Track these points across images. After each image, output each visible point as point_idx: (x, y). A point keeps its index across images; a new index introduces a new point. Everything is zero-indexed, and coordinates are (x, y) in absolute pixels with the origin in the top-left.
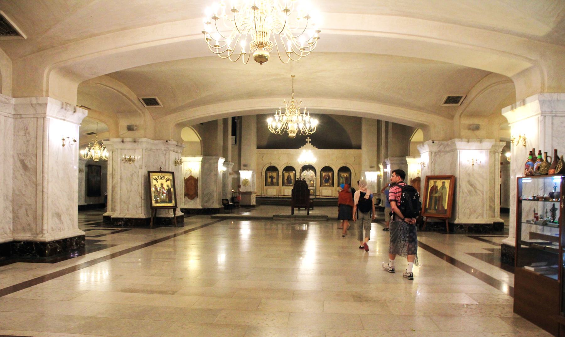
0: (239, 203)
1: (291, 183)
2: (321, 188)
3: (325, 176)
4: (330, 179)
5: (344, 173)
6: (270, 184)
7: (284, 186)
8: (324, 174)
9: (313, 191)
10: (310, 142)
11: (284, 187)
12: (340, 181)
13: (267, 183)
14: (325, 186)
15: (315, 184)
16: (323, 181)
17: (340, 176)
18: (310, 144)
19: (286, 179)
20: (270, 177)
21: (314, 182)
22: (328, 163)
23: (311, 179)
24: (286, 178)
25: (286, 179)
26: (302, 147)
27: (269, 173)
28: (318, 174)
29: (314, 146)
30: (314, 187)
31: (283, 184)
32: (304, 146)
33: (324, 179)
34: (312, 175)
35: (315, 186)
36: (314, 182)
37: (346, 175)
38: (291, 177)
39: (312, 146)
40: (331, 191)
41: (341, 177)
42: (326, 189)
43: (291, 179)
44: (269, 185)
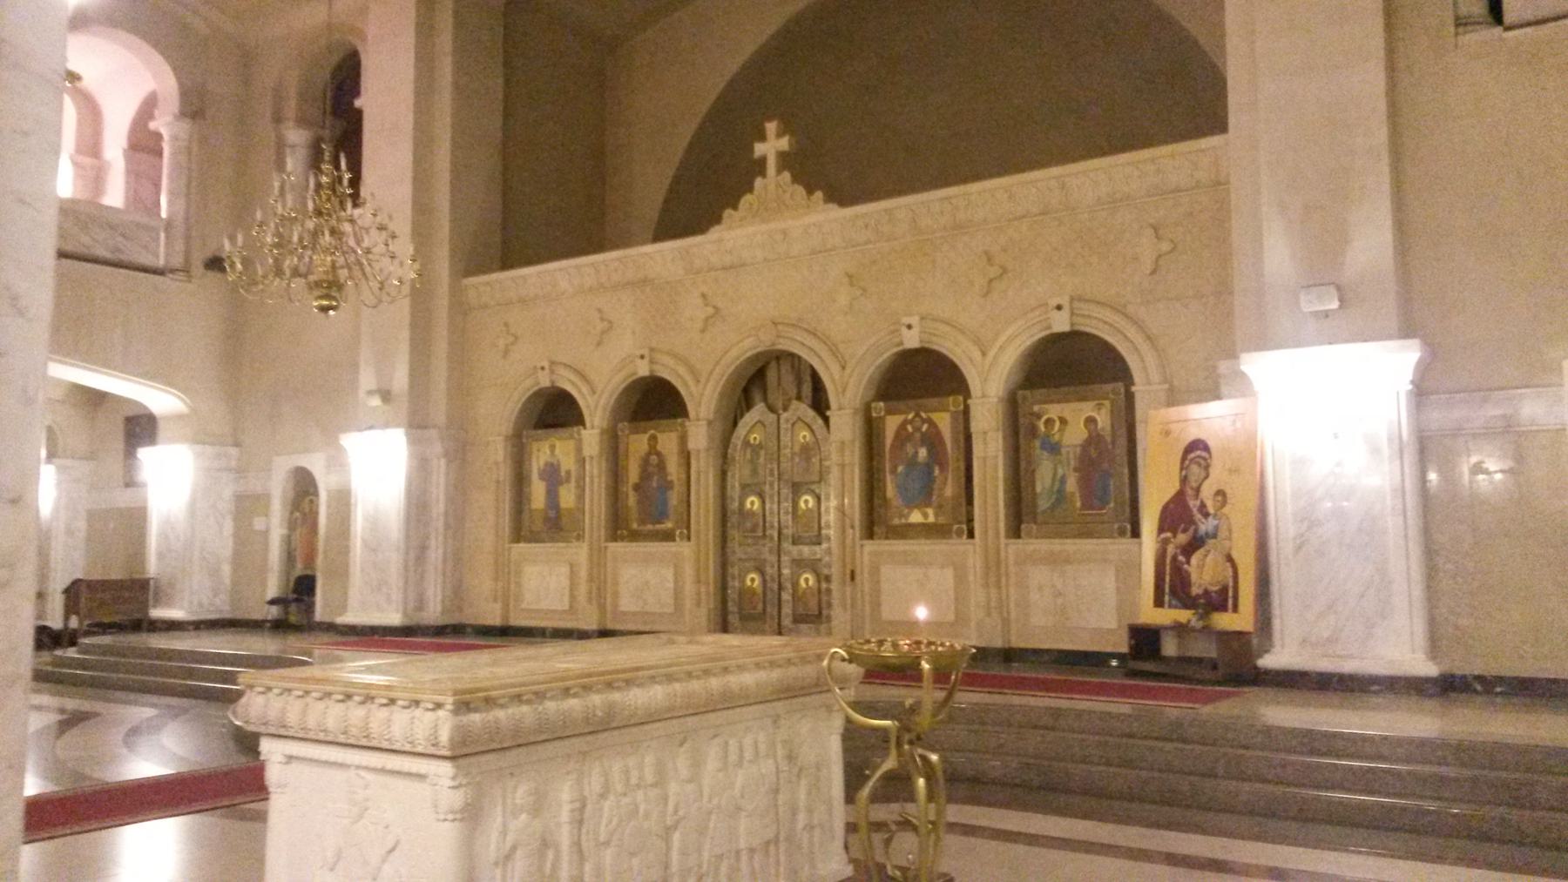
2: (870, 546)
3: (902, 437)
4: (943, 468)
5: (1065, 400)
6: (539, 525)
17: (1033, 431)
18: (787, 175)
19: (637, 488)
22: (914, 320)
24: (633, 474)
25: (637, 488)
26: (728, 212)
28: (845, 424)
29: (810, 192)
32: (747, 199)
33: (894, 471)
34: (804, 435)
37: (1091, 421)
38: (661, 466)
40: (949, 573)
41: (1037, 443)
43: (667, 486)
44: (534, 538)
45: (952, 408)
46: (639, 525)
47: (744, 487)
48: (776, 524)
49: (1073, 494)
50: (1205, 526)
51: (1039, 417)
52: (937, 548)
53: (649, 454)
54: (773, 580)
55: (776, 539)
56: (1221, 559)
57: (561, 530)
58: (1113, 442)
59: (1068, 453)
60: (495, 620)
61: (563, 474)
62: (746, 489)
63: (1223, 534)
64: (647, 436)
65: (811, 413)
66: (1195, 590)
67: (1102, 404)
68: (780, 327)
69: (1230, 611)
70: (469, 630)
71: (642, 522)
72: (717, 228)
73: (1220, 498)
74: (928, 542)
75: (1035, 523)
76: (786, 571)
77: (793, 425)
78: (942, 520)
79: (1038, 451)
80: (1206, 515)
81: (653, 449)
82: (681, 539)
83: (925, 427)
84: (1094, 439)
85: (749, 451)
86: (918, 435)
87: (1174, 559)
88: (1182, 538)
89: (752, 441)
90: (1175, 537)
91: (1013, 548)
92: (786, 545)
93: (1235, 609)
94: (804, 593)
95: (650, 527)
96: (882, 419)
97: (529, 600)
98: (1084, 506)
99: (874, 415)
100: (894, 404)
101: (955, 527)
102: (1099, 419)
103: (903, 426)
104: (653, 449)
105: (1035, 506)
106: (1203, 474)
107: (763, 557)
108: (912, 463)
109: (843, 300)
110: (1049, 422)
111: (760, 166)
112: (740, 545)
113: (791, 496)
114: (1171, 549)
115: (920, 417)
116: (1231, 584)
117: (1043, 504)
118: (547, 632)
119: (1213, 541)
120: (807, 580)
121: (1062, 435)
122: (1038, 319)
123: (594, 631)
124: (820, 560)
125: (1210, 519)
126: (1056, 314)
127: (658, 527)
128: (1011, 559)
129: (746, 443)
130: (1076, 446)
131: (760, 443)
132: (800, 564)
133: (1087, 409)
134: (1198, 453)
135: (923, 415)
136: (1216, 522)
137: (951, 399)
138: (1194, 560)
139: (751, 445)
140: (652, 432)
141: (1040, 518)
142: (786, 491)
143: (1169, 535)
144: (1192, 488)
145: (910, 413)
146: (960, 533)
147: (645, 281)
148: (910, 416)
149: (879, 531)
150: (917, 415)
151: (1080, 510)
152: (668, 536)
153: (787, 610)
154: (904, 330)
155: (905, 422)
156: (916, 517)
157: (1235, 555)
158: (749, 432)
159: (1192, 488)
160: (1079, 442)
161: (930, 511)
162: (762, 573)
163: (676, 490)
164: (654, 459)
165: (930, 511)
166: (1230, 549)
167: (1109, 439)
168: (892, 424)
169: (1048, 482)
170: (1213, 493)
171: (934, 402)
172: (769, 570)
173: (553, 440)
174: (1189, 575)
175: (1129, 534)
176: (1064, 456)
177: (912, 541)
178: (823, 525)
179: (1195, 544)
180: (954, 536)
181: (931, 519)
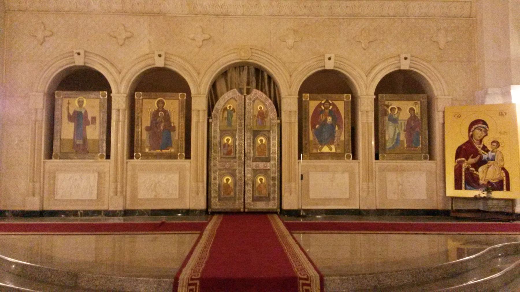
1: (168, 144)
3: (318, 112)
8: (313, 105)
12: (384, 134)
13: (57, 143)
14: (320, 156)
16: (311, 137)
17: (385, 113)
19: (148, 129)
20: (71, 118)
23: (255, 129)
24: (146, 121)
25: (148, 129)
27: (66, 101)
33: (313, 127)
34: (260, 107)
36: (268, 139)
37: (412, 110)
38: (167, 117)
40: (346, 175)
41: (387, 118)
42: (326, 170)
43: (170, 128)
44: (65, 156)
45: (345, 100)
46: (150, 150)
47: (222, 131)
48: (243, 152)
49: (403, 141)
50: (485, 157)
51: (388, 106)
52: (340, 164)
53: (157, 111)
54: (241, 180)
55: (243, 159)
56: (498, 170)
57: (88, 152)
58: (422, 119)
59: (401, 123)
60: (37, 207)
61: (89, 118)
62: (223, 133)
63: (498, 158)
64: (157, 100)
66: (482, 182)
67: (417, 103)
68: (253, 51)
69: (505, 190)
70: (7, 214)
71: (152, 148)
73: (495, 144)
74: (333, 161)
75: (386, 153)
76: (248, 175)
77: (254, 101)
78: (339, 151)
79: (387, 122)
80: (487, 151)
82: (181, 158)
83: (331, 108)
84: (413, 117)
85: (226, 113)
86: (327, 111)
87: (467, 169)
88: (472, 160)
89: (228, 108)
90: (467, 160)
91: (377, 165)
92: (248, 162)
93: (508, 189)
94: (259, 186)
95: (159, 151)
96: (308, 102)
97: (60, 194)
98: (408, 146)
99: (303, 99)
100: (315, 95)
101: (346, 154)
102: (415, 109)
105: (385, 145)
106: (484, 134)
107: (234, 168)
109: (290, 42)
110: (393, 109)
112: (219, 162)
113: (252, 137)
114: (464, 166)
115: (329, 103)
116: (505, 179)
117: (389, 145)
118: (79, 213)
119: (492, 162)
120: (261, 180)
121: (398, 116)
122: (394, 62)
123: (120, 211)
124: (269, 170)
125: (490, 153)
126: (403, 61)
127: (164, 151)
128: (377, 168)
129: (225, 109)
130: (405, 120)
131: (233, 109)
132: (256, 172)
133: (410, 104)
134: (480, 125)
135: (331, 102)
136: (493, 154)
137: (345, 95)
138: (480, 169)
139: (228, 110)
141: (388, 151)
142: (248, 135)
143: (463, 159)
144: (477, 140)
145: (323, 100)
146: (348, 157)
147: (159, 14)
148: (323, 102)
149: (306, 156)
150: (327, 101)
151: (406, 148)
152: (172, 156)
153: (249, 195)
155: (320, 104)
156: (326, 149)
157: (506, 167)
159: (477, 140)
160: (407, 119)
161: (333, 147)
162: (233, 175)
163: (177, 131)
165: (333, 147)
166: (504, 165)
167: (419, 118)
168: (313, 105)
169: (391, 136)
170: (491, 142)
171: (337, 96)
173: (81, 98)
174: (478, 176)
175: (428, 159)
176: (399, 124)
177: (324, 161)
178: (271, 152)
179: (482, 162)
180: (346, 159)
181: (334, 150)
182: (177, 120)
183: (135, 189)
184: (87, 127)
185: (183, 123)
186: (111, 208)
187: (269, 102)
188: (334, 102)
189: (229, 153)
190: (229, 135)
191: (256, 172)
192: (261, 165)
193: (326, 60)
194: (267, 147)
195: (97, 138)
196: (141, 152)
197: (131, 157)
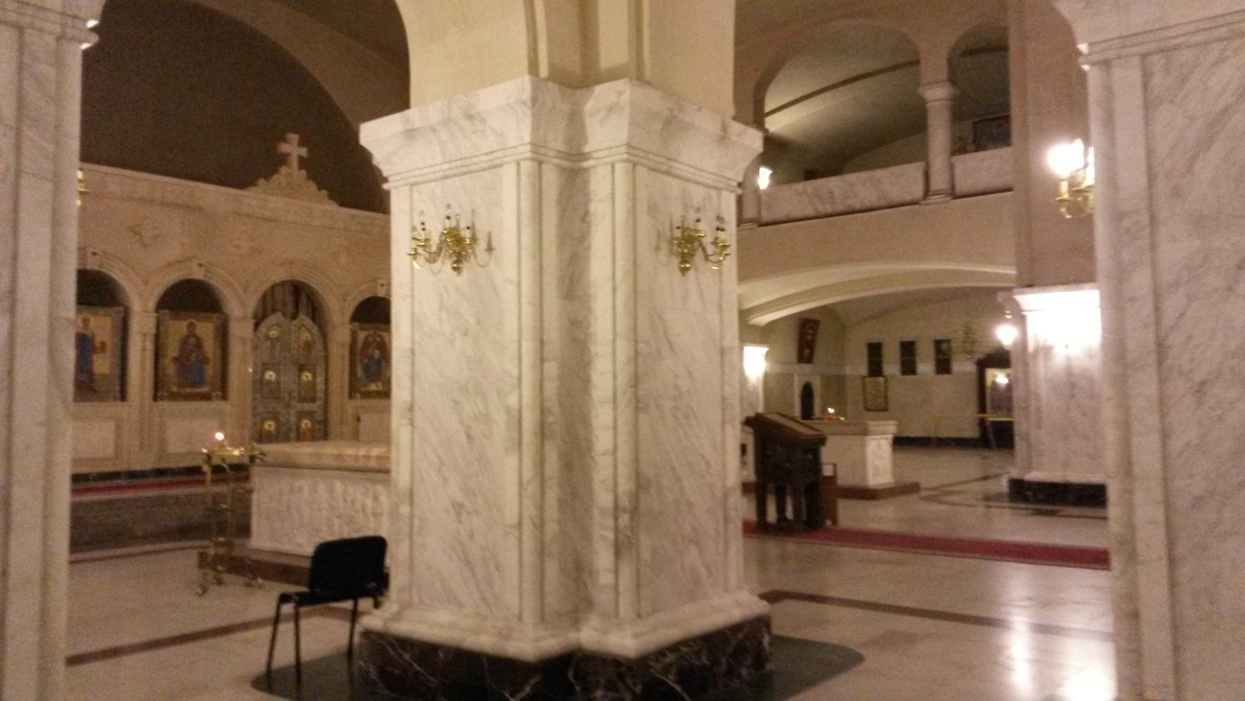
0: (203, 561)
3: (366, 344)
7: (162, 399)
8: (362, 336)
9: (313, 421)
10: (303, 163)
11: (165, 405)
15: (320, 386)
18: (304, 173)
21: (314, 375)
24: (172, 350)
25: (176, 360)
26: (261, 181)
29: (319, 189)
30: (319, 403)
31: (159, 390)
34: (306, 336)
35: (320, 395)
38: (199, 345)
39: (313, 186)
43: (204, 360)
61: (98, 344)
65: (310, 322)
71: (180, 386)
72: (253, 189)
81: (192, 333)
95: (188, 390)
103: (367, 338)
104: (192, 333)
108: (371, 358)
111: (283, 159)
132: (301, 415)
140: (191, 320)
152: (206, 397)
154: (379, 287)
155: (369, 335)
156: (373, 387)
158: (269, 329)
162: (276, 419)
163: (211, 365)
164: (192, 340)
172: (282, 419)
182: (210, 348)
183: (163, 441)
184: (95, 357)
185: (219, 353)
186: (138, 467)
187: (315, 329)
188: (381, 333)
189: (271, 392)
190: (273, 370)
191: (301, 415)
192: (307, 406)
193: (379, 287)
194: (313, 385)
195: (107, 372)
196: (168, 392)
197: (155, 398)
